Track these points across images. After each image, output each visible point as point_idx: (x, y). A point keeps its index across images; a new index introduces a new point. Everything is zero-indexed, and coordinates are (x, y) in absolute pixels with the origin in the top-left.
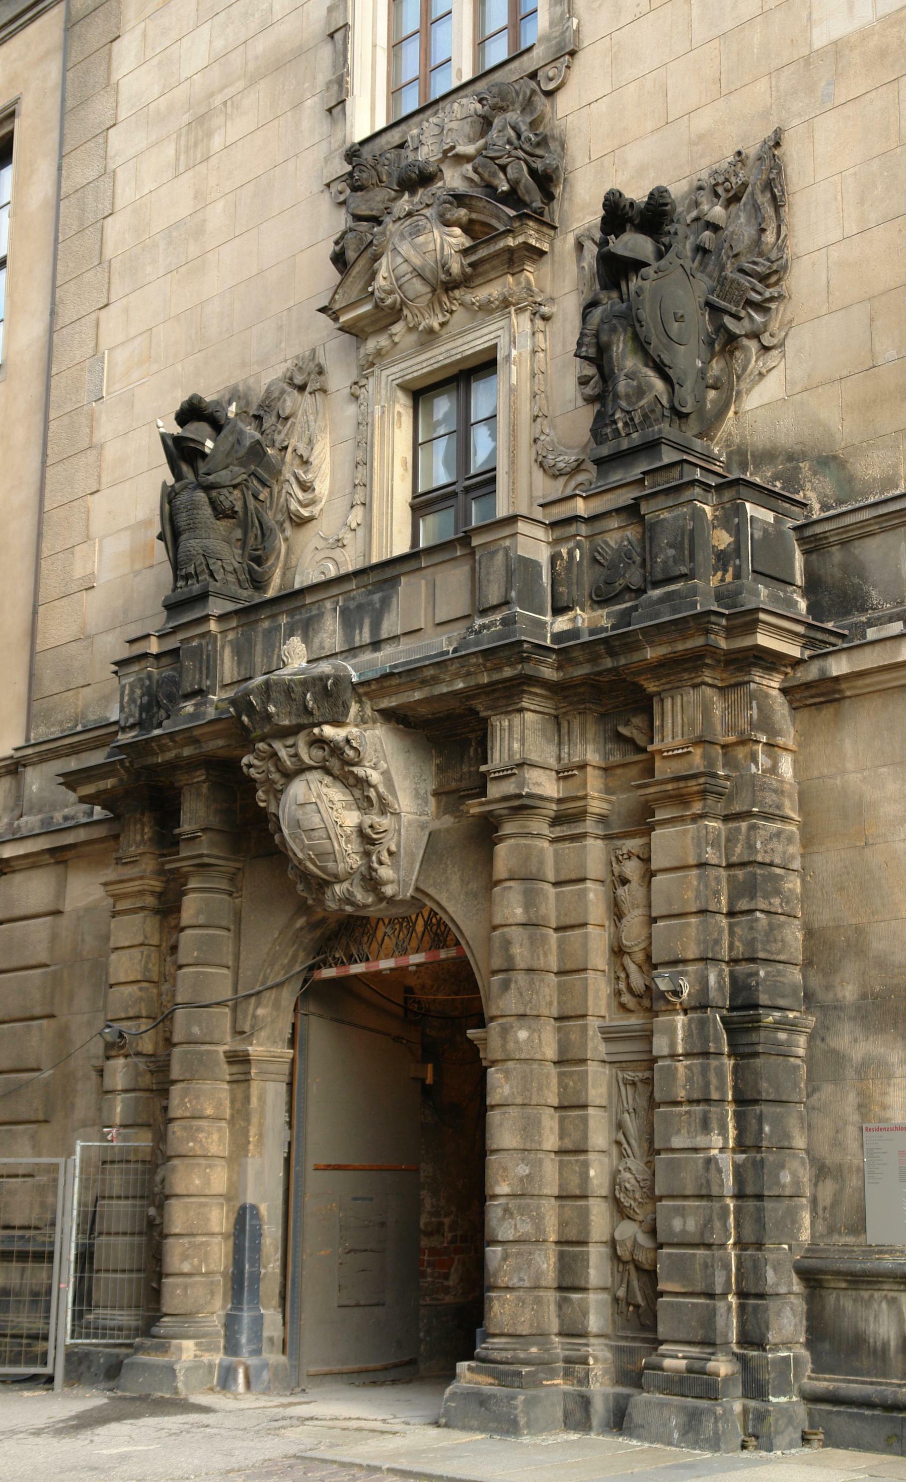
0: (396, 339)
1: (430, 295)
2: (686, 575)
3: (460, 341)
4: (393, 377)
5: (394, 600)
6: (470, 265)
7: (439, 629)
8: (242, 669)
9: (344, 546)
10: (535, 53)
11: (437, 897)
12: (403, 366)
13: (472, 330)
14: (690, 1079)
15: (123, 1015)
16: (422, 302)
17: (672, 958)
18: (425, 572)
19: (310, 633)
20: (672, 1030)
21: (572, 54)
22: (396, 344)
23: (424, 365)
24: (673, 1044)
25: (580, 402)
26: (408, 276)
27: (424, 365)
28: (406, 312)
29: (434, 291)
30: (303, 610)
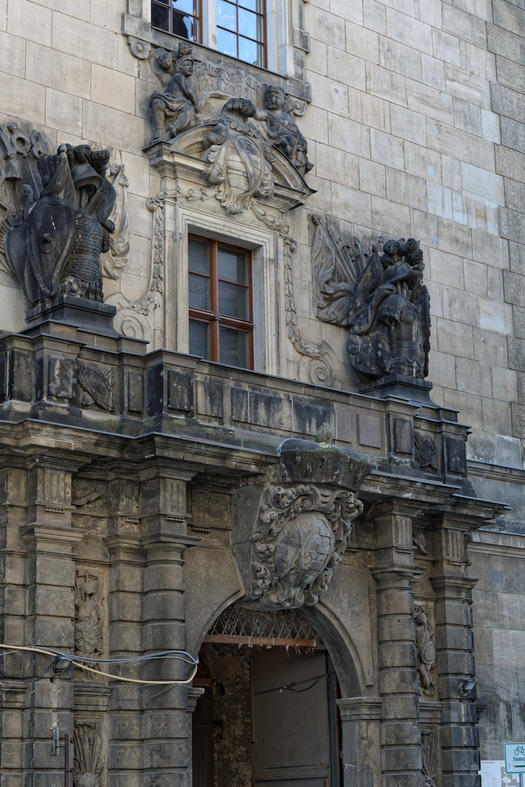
0: (205, 198)
1: (243, 192)
2: (462, 473)
3: (239, 227)
4: (188, 218)
5: (332, 415)
6: (276, 195)
7: (360, 447)
8: (215, 408)
9: (147, 315)
10: (288, 82)
11: (334, 610)
12: (195, 214)
13: (249, 226)
14: (468, 735)
15: (57, 644)
16: (237, 192)
17: (458, 672)
18: (350, 407)
19: (272, 409)
20: (459, 710)
21: (308, 103)
22: (202, 199)
23: (212, 225)
24: (460, 717)
25: (313, 316)
26: (241, 173)
27: (212, 225)
28: (222, 188)
29: (247, 191)
30: (262, 388)
